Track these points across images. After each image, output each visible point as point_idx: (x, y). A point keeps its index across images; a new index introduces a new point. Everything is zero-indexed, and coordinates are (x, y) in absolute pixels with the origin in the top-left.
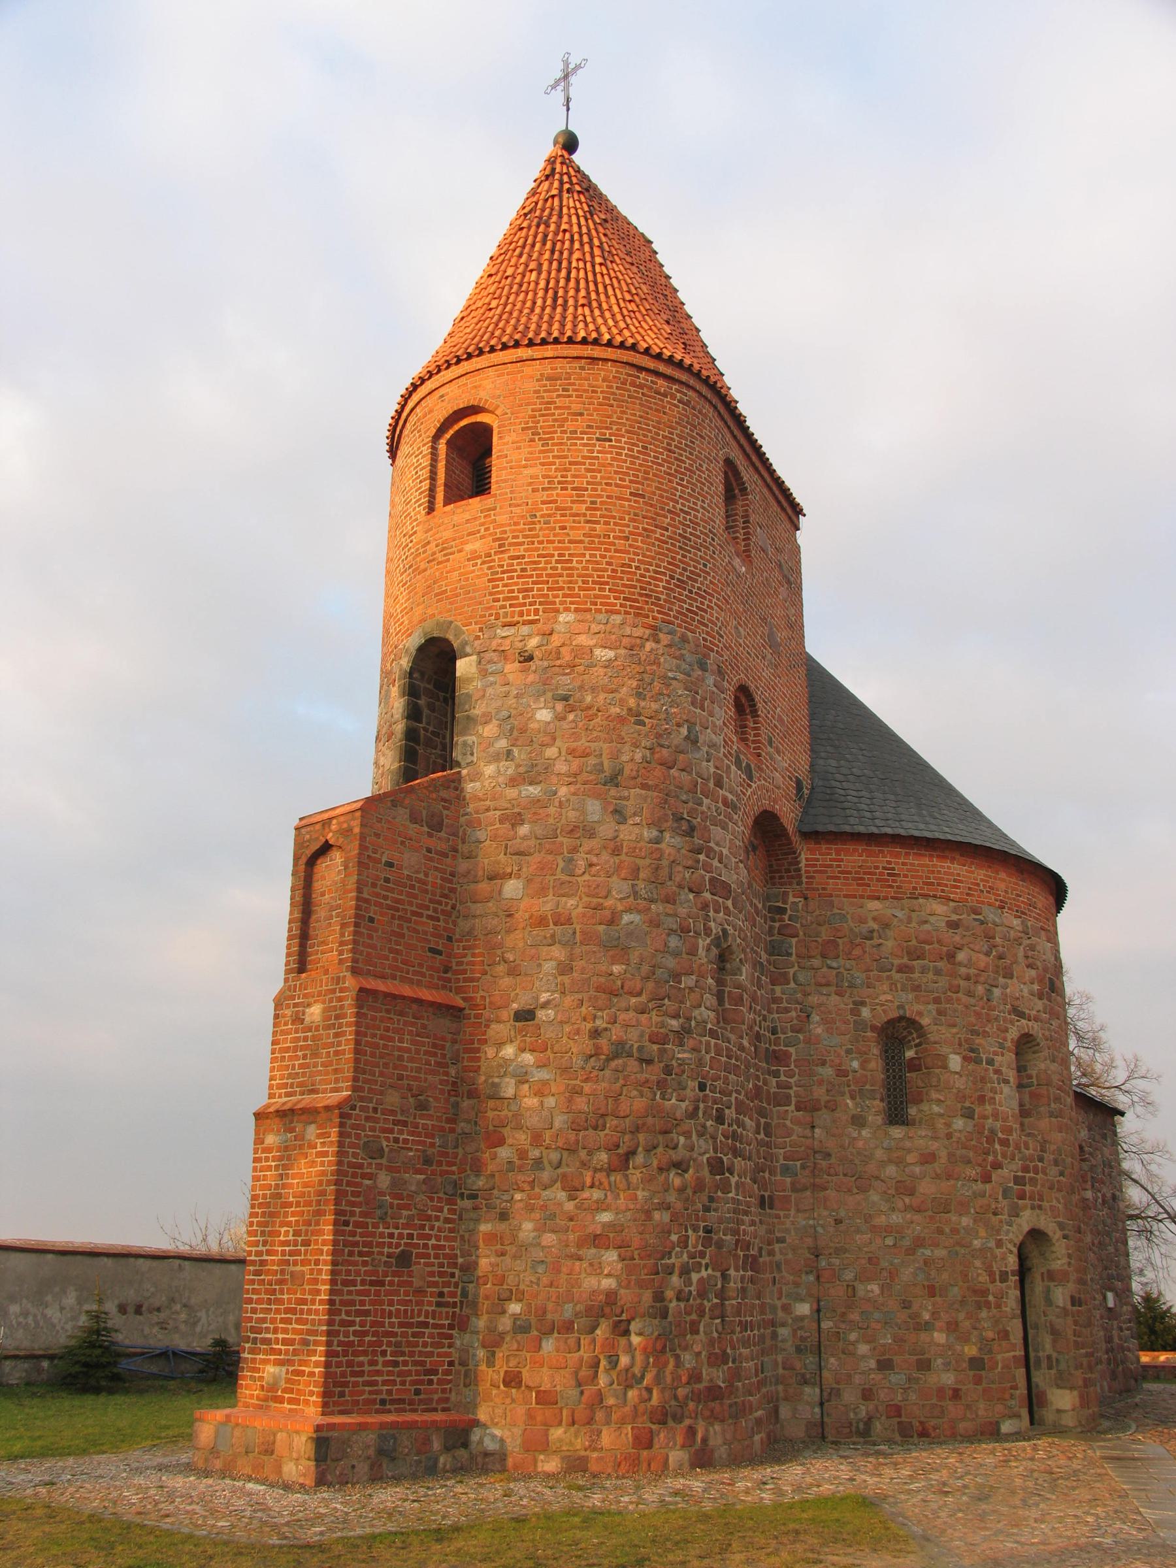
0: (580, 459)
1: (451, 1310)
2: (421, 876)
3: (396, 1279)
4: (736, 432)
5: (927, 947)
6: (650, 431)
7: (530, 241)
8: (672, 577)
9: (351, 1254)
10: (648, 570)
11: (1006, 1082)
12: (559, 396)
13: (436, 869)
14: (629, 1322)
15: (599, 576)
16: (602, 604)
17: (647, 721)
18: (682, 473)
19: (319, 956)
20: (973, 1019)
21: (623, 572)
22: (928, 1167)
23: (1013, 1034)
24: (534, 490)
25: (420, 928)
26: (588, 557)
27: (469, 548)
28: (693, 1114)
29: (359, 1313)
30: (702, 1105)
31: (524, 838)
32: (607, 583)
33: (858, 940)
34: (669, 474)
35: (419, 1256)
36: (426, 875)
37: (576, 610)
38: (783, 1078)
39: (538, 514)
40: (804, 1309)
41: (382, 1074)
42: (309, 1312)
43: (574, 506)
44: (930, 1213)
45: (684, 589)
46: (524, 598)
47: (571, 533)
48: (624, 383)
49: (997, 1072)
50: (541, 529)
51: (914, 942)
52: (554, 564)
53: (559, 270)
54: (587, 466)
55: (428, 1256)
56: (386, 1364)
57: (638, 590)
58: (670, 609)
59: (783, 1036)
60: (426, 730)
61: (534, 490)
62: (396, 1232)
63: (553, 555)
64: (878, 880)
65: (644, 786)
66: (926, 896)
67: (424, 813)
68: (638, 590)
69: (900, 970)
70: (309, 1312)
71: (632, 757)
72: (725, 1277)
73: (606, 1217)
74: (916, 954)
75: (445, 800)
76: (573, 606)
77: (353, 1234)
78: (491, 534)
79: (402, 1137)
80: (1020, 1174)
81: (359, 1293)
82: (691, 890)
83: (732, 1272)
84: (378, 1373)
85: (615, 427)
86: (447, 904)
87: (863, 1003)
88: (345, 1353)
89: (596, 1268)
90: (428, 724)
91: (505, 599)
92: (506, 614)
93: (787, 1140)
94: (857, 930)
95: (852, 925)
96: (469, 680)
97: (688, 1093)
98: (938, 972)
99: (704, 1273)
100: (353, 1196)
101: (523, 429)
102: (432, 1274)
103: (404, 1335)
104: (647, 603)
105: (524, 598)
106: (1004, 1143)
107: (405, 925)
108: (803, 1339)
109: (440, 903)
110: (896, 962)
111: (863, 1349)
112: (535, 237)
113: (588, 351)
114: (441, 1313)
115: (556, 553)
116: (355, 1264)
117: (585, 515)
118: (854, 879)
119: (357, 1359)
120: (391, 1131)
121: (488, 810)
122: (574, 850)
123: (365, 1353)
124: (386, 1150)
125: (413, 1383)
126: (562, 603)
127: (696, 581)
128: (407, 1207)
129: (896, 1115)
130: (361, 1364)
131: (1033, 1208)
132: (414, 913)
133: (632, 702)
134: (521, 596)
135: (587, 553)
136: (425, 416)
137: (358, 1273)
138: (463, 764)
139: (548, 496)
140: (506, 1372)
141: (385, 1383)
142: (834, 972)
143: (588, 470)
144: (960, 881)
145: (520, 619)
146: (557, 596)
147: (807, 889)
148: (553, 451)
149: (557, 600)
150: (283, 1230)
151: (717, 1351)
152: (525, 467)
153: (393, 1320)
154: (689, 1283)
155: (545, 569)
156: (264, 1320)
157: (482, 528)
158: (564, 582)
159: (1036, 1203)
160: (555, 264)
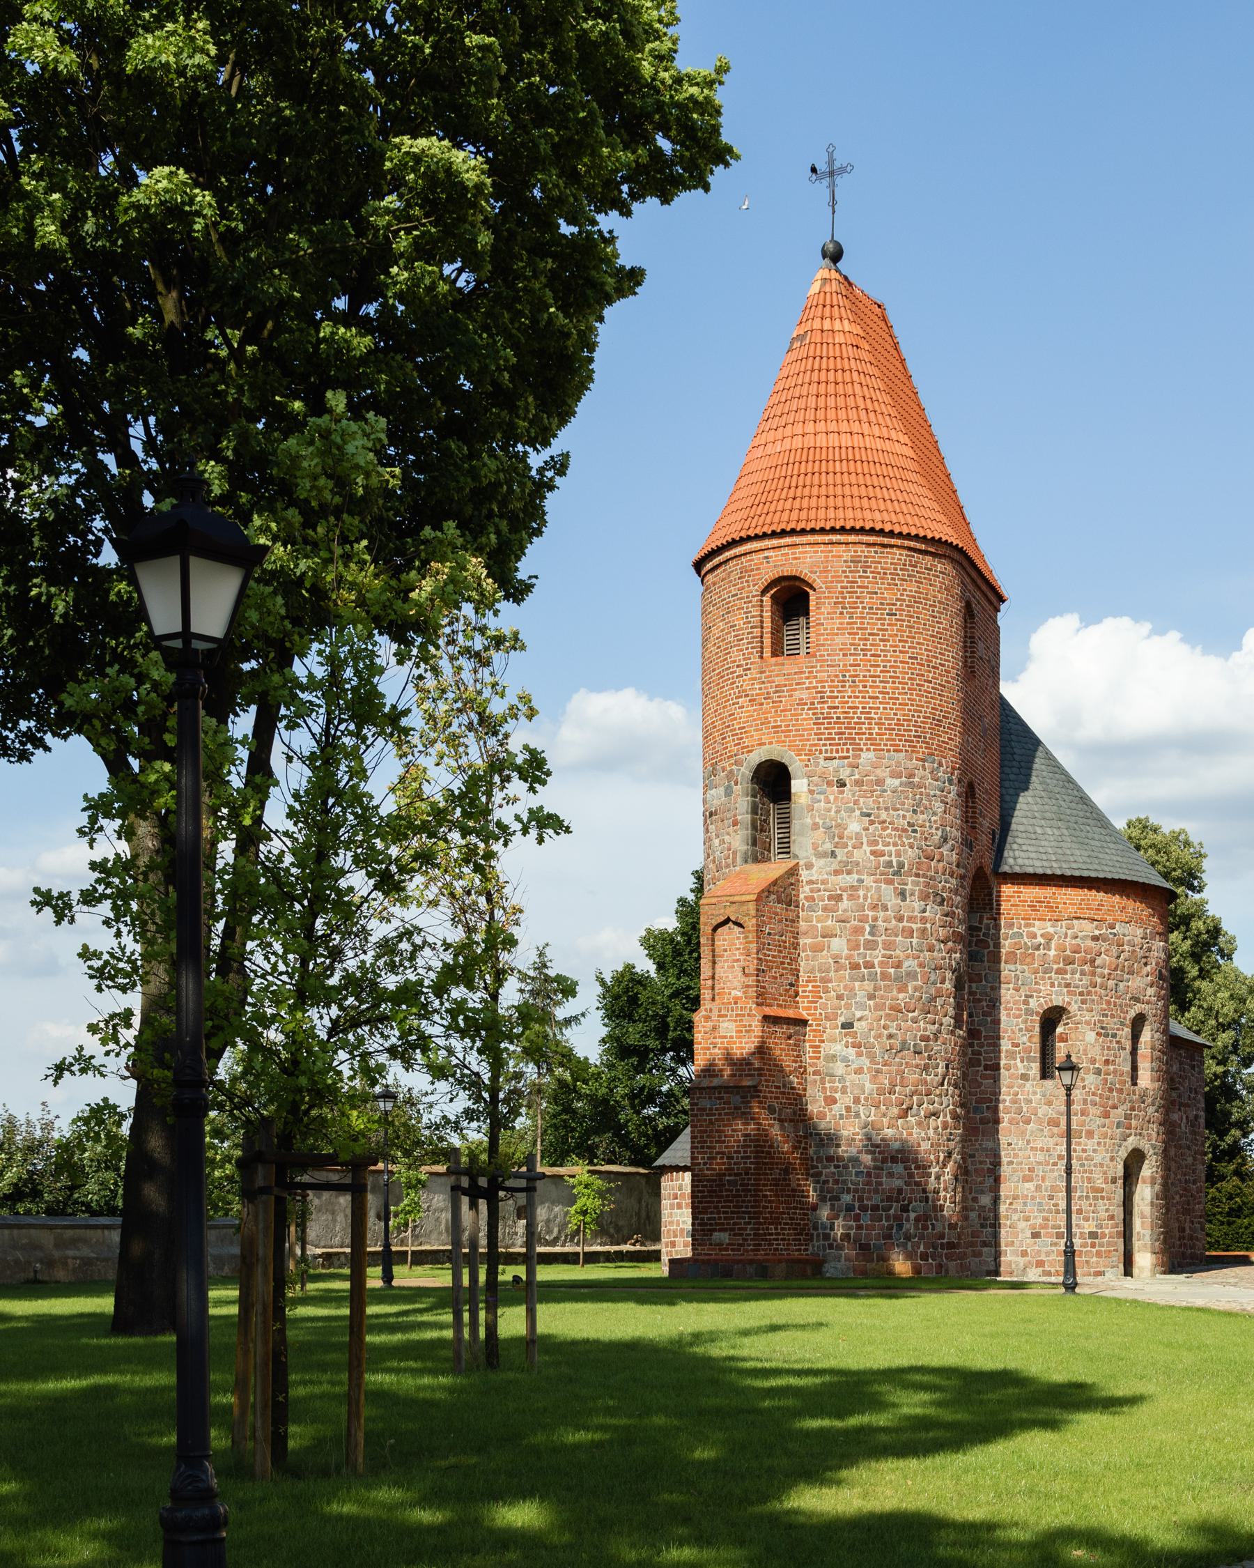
23: (1132, 1014)
24: (845, 655)
31: (844, 911)
42: (743, 1201)
49: (1118, 1042)
51: (1068, 952)
61: (845, 655)
65: (917, 875)
69: (1058, 972)
70: (743, 1201)
71: (910, 855)
87: (1031, 996)
89: (891, 1175)
91: (826, 739)
92: (826, 751)
97: (940, 1070)
98: (1083, 973)
106: (1120, 1091)
108: (985, 1219)
110: (1055, 967)
111: (1022, 1224)
122: (876, 919)
143: (881, 640)
146: (861, 739)
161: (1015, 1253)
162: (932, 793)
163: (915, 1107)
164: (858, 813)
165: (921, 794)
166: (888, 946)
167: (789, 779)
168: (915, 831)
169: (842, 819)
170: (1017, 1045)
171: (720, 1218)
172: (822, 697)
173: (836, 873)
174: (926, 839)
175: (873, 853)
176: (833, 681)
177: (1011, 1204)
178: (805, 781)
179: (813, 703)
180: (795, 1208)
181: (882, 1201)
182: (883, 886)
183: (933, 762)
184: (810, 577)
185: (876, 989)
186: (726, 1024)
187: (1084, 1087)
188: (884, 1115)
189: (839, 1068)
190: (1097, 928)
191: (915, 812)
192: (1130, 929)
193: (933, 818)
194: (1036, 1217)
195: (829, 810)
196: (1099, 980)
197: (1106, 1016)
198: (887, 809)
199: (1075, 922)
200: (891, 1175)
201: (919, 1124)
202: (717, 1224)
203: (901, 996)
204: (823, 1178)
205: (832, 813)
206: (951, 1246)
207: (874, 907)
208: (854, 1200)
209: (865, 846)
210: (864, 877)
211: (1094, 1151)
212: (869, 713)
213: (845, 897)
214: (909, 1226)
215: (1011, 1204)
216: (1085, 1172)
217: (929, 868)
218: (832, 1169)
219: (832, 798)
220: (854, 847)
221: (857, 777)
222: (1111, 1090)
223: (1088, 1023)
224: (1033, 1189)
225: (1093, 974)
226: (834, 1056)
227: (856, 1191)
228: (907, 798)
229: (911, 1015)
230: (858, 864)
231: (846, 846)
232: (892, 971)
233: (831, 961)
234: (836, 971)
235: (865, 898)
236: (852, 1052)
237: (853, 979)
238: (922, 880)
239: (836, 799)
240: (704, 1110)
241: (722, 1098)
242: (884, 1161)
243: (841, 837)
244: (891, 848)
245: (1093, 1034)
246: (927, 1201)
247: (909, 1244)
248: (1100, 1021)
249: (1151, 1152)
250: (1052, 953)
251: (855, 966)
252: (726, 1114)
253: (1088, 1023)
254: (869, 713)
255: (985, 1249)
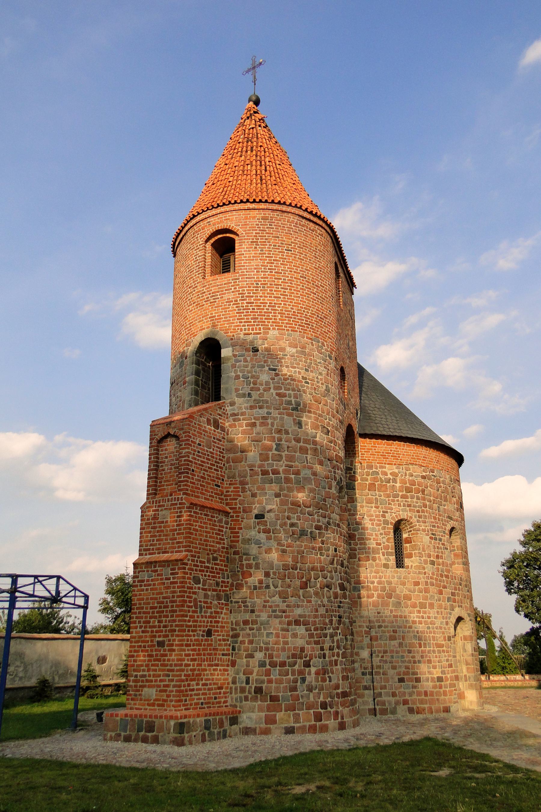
0: (278, 259)
1: (227, 657)
2: (211, 450)
3: (206, 643)
4: (337, 250)
5: (413, 487)
6: (308, 248)
7: (244, 149)
8: (318, 316)
9: (189, 631)
10: (308, 312)
11: (447, 549)
12: (267, 228)
13: (217, 447)
14: (310, 661)
15: (287, 314)
16: (289, 327)
17: (310, 382)
18: (321, 268)
19: (165, 487)
20: (433, 520)
21: (298, 313)
22: (417, 587)
23: (449, 527)
24: (257, 272)
25: (212, 475)
26: (282, 305)
27: (226, 297)
28: (332, 563)
29: (192, 660)
30: (336, 559)
31: (258, 433)
32: (292, 318)
33: (384, 483)
34: (316, 268)
35: (215, 631)
36: (213, 450)
37: (278, 329)
38: (352, 546)
39: (259, 283)
40: (365, 654)
41: (199, 544)
42: (169, 660)
43: (276, 280)
44: (418, 609)
45: (323, 322)
46: (254, 322)
47: (275, 293)
48: (296, 224)
49: (443, 544)
50: (261, 290)
51: (408, 485)
52: (267, 307)
53: (261, 165)
54: (281, 262)
55: (218, 631)
56: (203, 685)
57: (304, 322)
58: (318, 331)
59: (352, 527)
60: (202, 380)
61: (258, 272)
62: (206, 620)
63: (267, 303)
64: (392, 456)
66: (412, 464)
67: (212, 420)
68: (304, 322)
70: (169, 660)
72: (346, 639)
73: (298, 611)
74: (409, 490)
75: (220, 415)
76: (276, 328)
77: (189, 621)
78: (237, 291)
79: (207, 574)
80: (453, 591)
81: (192, 650)
82: (329, 460)
83: (348, 637)
84: (200, 689)
85: (293, 245)
86: (221, 464)
87: (387, 512)
88: (187, 680)
89: (295, 636)
90: (203, 378)
91: (245, 322)
92: (245, 330)
93: (355, 575)
94: (383, 479)
95: (381, 476)
96: (228, 359)
97: (330, 552)
98: (418, 498)
99: (339, 637)
100: (189, 603)
101: (251, 242)
102: (220, 640)
103: (210, 670)
104: (308, 328)
105: (254, 322)
107: (206, 473)
108: (365, 668)
109: (219, 463)
110: (400, 494)
111: (391, 672)
112: (247, 147)
113: (280, 207)
114: (224, 659)
115: (268, 302)
116: (190, 636)
117: (281, 285)
118: (381, 455)
119: (192, 683)
120: (203, 571)
121: (240, 420)
123: (194, 680)
124: (202, 580)
125: (214, 694)
126: (271, 326)
127: (327, 318)
128: (210, 608)
129: (400, 564)
130: (193, 686)
131: (459, 607)
132: (209, 468)
133: (303, 371)
134: (252, 321)
135: (282, 303)
136: (199, 230)
137: (191, 640)
138: (226, 398)
139: (264, 275)
140: (255, 687)
141: (203, 694)
142: (374, 497)
144: (426, 458)
145: (252, 332)
146: (269, 322)
147: (361, 459)
148: (265, 254)
149: (269, 324)
150: (152, 620)
151: (345, 674)
152: (253, 260)
153: (205, 663)
154: (333, 642)
155: (264, 309)
156: (142, 666)
157: (233, 288)
158: (272, 316)
159: (460, 604)
160: (259, 162)
161: (387, 694)
162: (318, 361)
163: (312, 580)
164: (267, 368)
165: (311, 359)
166: (290, 458)
167: (221, 349)
168: (307, 383)
169: (256, 372)
170: (380, 544)
171: (150, 676)
172: (242, 297)
173: (252, 407)
174: (315, 389)
175: (278, 395)
176: (249, 287)
177: (382, 657)
178: (231, 349)
179: (236, 301)
180: (217, 665)
181: (288, 658)
182: (286, 417)
183: (318, 342)
184: (235, 228)
185: (281, 489)
186: (164, 512)
187: (425, 573)
188: (289, 586)
189: (254, 550)
190: (424, 471)
191: (306, 370)
192: (443, 473)
193: (319, 377)
194: (400, 667)
195: (247, 366)
196: (428, 503)
197: (434, 526)
198: (287, 367)
199: (410, 466)
200: (295, 636)
201: (316, 594)
202: (147, 681)
203: (300, 495)
204: (240, 639)
205: (249, 368)
206: (345, 694)
207: (279, 431)
208: (265, 657)
209: (272, 390)
210: (272, 411)
211: (436, 618)
212: (275, 306)
213: (258, 424)
214: (311, 678)
215: (382, 657)
216: (430, 632)
217: (318, 408)
218: (248, 631)
219: (249, 359)
220: (264, 390)
221: (266, 346)
222: (442, 576)
223: (424, 530)
224: (397, 645)
225: (424, 499)
226: (249, 540)
227: (267, 649)
228: (301, 361)
229: (307, 509)
230: (267, 402)
231: (259, 389)
232: (293, 476)
233: (248, 469)
234: (251, 476)
235: (272, 424)
236: (263, 536)
237: (264, 482)
238: (313, 415)
239: (252, 360)
240: (143, 581)
241: (157, 571)
242: (289, 624)
243: (255, 383)
244: (290, 392)
245: (428, 537)
246: (324, 658)
247: (311, 695)
248: (431, 530)
249: (469, 618)
250: (398, 485)
251: (265, 473)
252: (159, 584)
253: (424, 530)
254: (273, 306)
255: (366, 692)
